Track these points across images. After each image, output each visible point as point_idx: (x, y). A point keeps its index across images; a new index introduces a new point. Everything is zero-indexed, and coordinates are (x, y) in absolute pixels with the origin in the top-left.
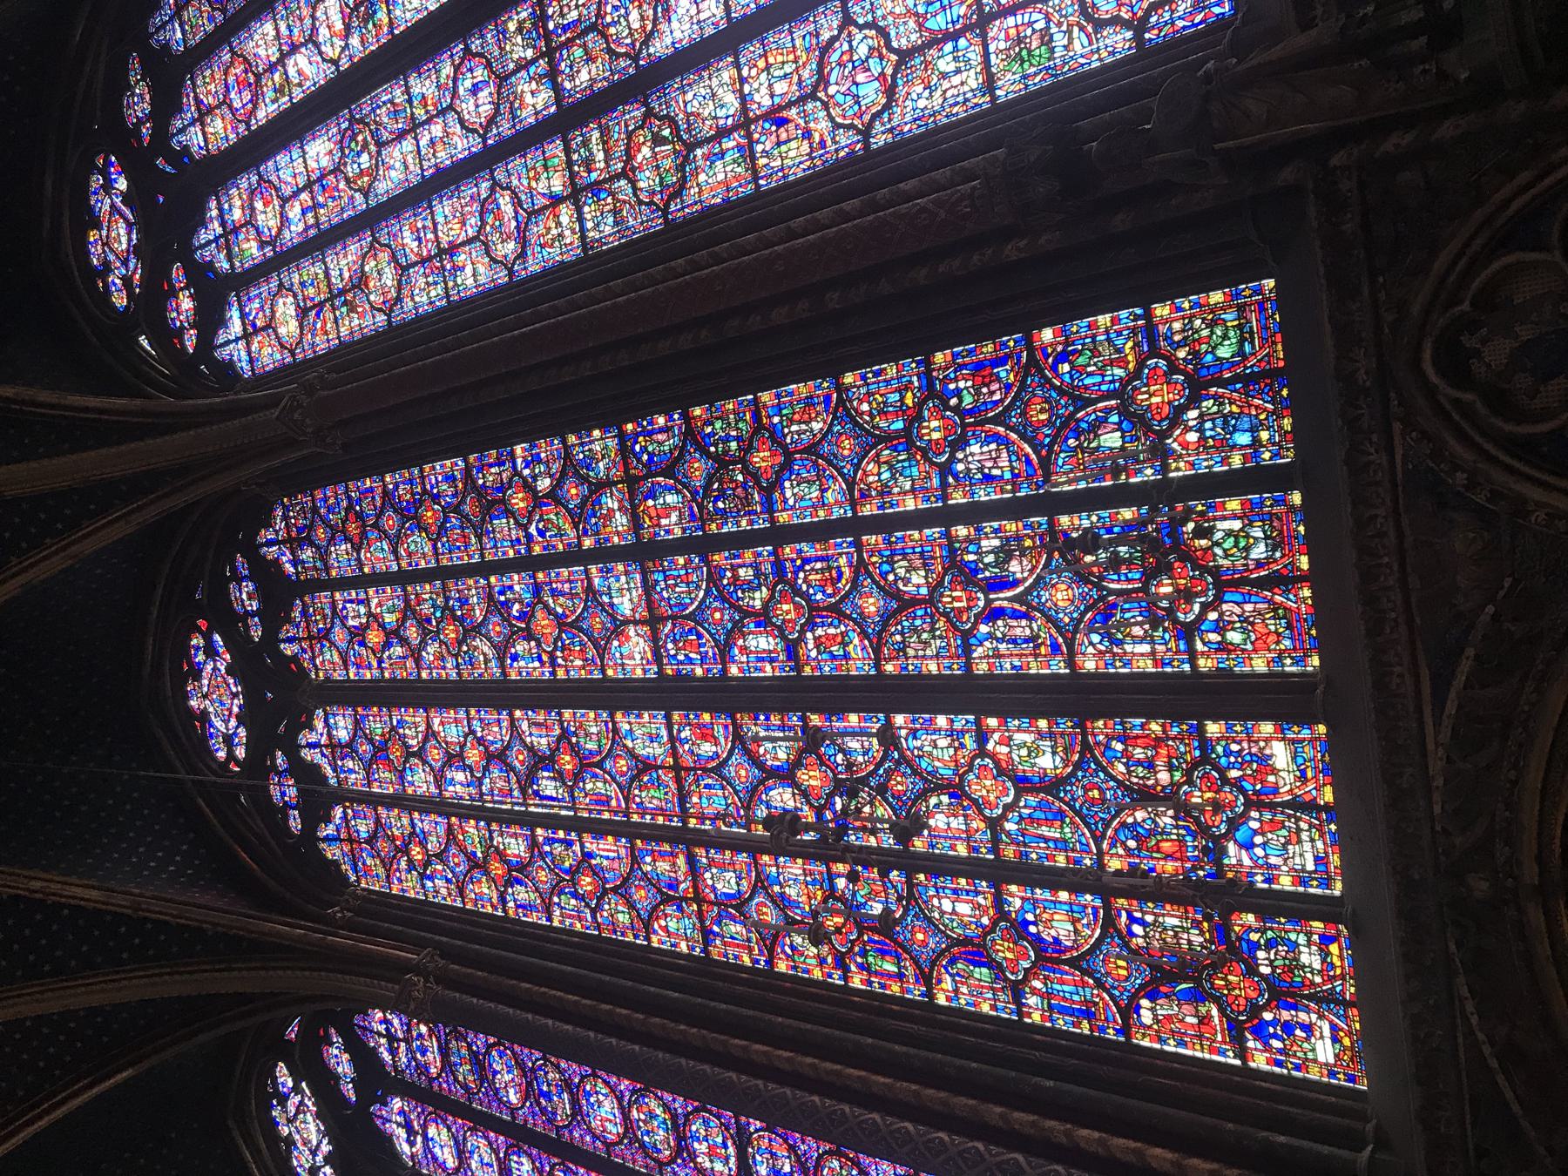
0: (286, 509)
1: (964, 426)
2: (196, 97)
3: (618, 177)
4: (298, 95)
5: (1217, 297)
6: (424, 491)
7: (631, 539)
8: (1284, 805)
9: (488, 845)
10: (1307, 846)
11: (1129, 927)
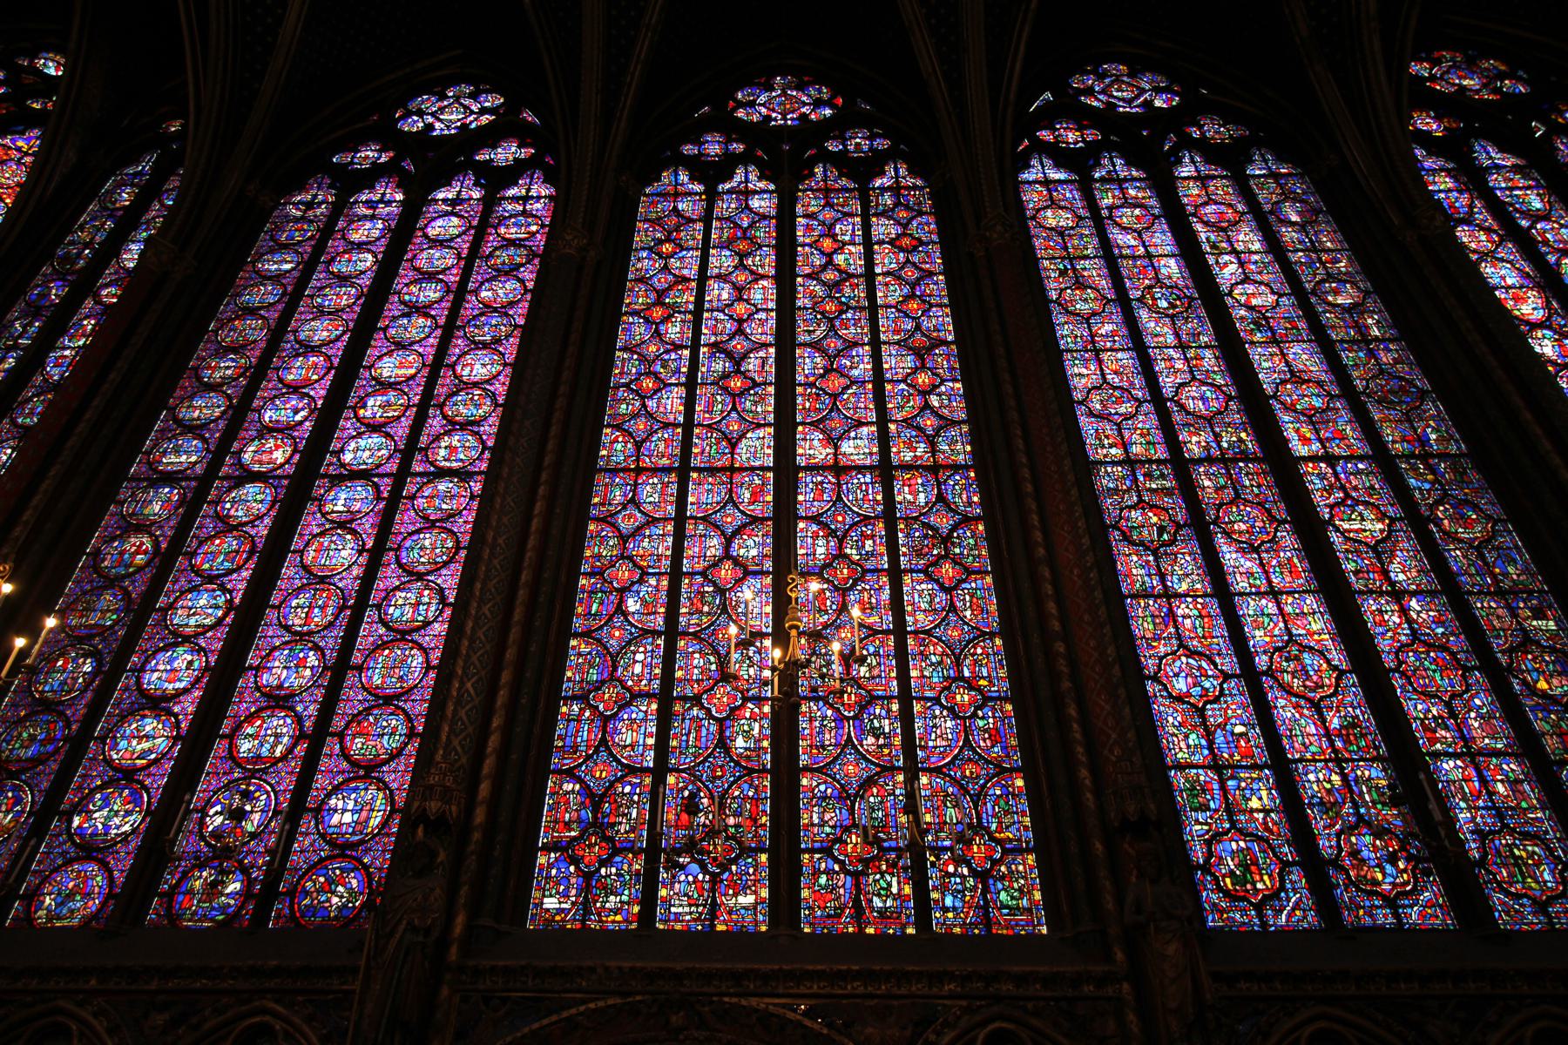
0: (921, 189)
1: (964, 718)
2: (1214, 177)
3: (1139, 496)
4: (1211, 260)
5: (1038, 896)
6: (931, 306)
7: (895, 461)
8: (714, 898)
9: (674, 309)
10: (687, 909)
11: (630, 783)
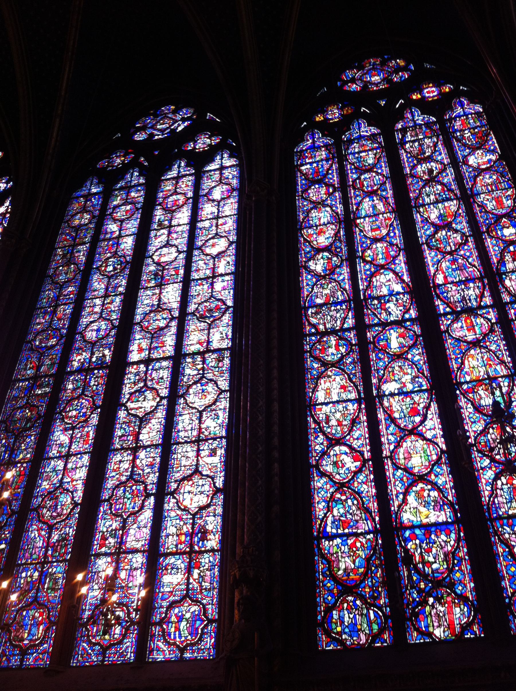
3: (27, 400)
